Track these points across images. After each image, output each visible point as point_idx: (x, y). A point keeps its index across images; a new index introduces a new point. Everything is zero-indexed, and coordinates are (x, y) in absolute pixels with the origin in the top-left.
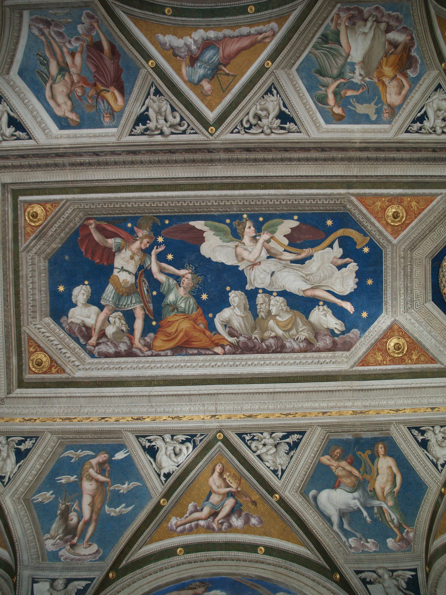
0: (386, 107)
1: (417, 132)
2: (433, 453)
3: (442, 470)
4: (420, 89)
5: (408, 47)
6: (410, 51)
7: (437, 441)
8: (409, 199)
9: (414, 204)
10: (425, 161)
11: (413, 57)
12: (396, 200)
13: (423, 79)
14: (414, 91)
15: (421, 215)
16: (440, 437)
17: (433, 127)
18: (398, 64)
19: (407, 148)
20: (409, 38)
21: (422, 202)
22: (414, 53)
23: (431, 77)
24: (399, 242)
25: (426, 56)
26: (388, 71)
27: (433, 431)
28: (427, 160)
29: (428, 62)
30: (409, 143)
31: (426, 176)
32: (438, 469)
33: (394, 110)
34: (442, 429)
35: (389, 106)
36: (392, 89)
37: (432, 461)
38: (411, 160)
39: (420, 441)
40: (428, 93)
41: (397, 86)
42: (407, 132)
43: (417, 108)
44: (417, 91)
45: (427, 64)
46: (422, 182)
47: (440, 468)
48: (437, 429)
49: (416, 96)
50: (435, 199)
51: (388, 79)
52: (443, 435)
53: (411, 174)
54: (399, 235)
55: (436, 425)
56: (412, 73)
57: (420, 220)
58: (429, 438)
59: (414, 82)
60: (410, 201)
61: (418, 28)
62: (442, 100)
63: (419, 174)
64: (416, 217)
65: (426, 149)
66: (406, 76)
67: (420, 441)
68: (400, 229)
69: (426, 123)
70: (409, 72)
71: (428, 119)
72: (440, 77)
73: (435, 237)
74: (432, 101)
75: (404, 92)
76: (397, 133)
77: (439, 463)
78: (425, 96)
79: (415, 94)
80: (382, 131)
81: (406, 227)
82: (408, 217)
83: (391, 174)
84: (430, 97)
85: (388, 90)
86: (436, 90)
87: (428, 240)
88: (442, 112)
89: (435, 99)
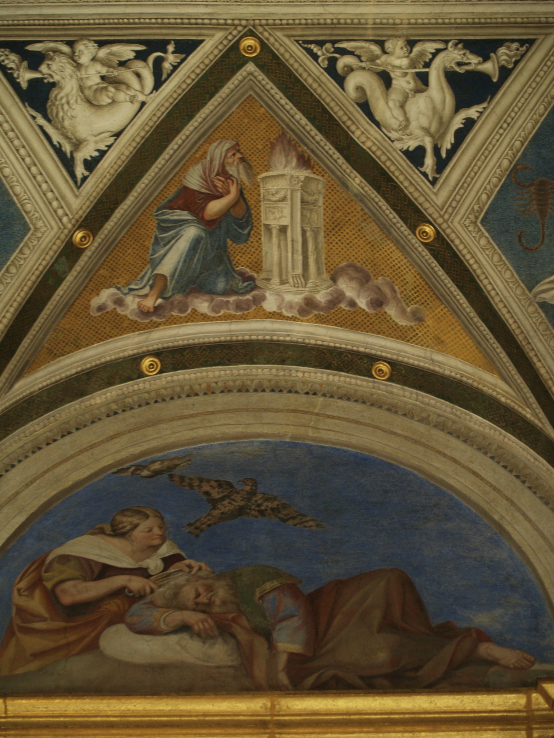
2: (67, 123)
3: (85, 179)
7: (81, 89)
16: (93, 75)
27: (72, 57)
32: (73, 175)
34: (103, 53)
37: (58, 151)
39: (24, 85)
47: (80, 170)
48: (86, 51)
52: (104, 71)
55: (83, 37)
58: (57, 78)
67: (24, 85)
77: (80, 156)
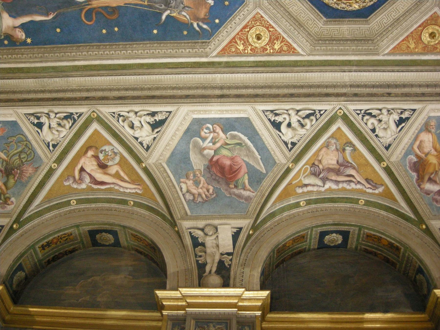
0: (433, 130)
1: (405, 110)
4: (404, 145)
5: (420, 179)
6: (418, 176)
8: (417, 50)
9: (412, 46)
10: (399, 85)
11: (414, 172)
12: (429, 49)
13: (402, 154)
14: (409, 144)
15: (406, 35)
17: (391, 114)
18: (425, 165)
19: (415, 96)
20: (422, 186)
21: (404, 47)
22: (414, 175)
23: (395, 156)
24: (432, 8)
25: (404, 172)
26: (433, 160)
28: (397, 86)
29: (401, 167)
30: (413, 101)
31: (398, 71)
33: (426, 128)
35: (430, 132)
36: (427, 145)
38: (412, 86)
40: (396, 143)
41: (423, 148)
42: (414, 110)
43: (405, 130)
44: (406, 144)
45: (401, 166)
46: (403, 66)
49: (406, 140)
50: (391, 50)
51: (432, 153)
53: (413, 73)
54: (431, 16)
56: (412, 159)
57: (408, 29)
59: (409, 151)
60: (416, 48)
61: (418, 194)
62: (383, 137)
63: (404, 73)
64: (412, 33)
65: (397, 95)
66: (417, 156)
68: (429, 22)
69: (397, 118)
70: (415, 159)
71: (395, 121)
72: (388, 156)
73: (394, 14)
74: (392, 136)
75: (418, 143)
76: (423, 109)
78: (398, 140)
79: (408, 142)
80: (436, 111)
81: (422, 24)
82: (419, 33)
83: (431, 73)
84: (395, 139)
85: (431, 145)
86: (390, 145)
87: (402, 11)
88: (382, 127)
89: (390, 138)
